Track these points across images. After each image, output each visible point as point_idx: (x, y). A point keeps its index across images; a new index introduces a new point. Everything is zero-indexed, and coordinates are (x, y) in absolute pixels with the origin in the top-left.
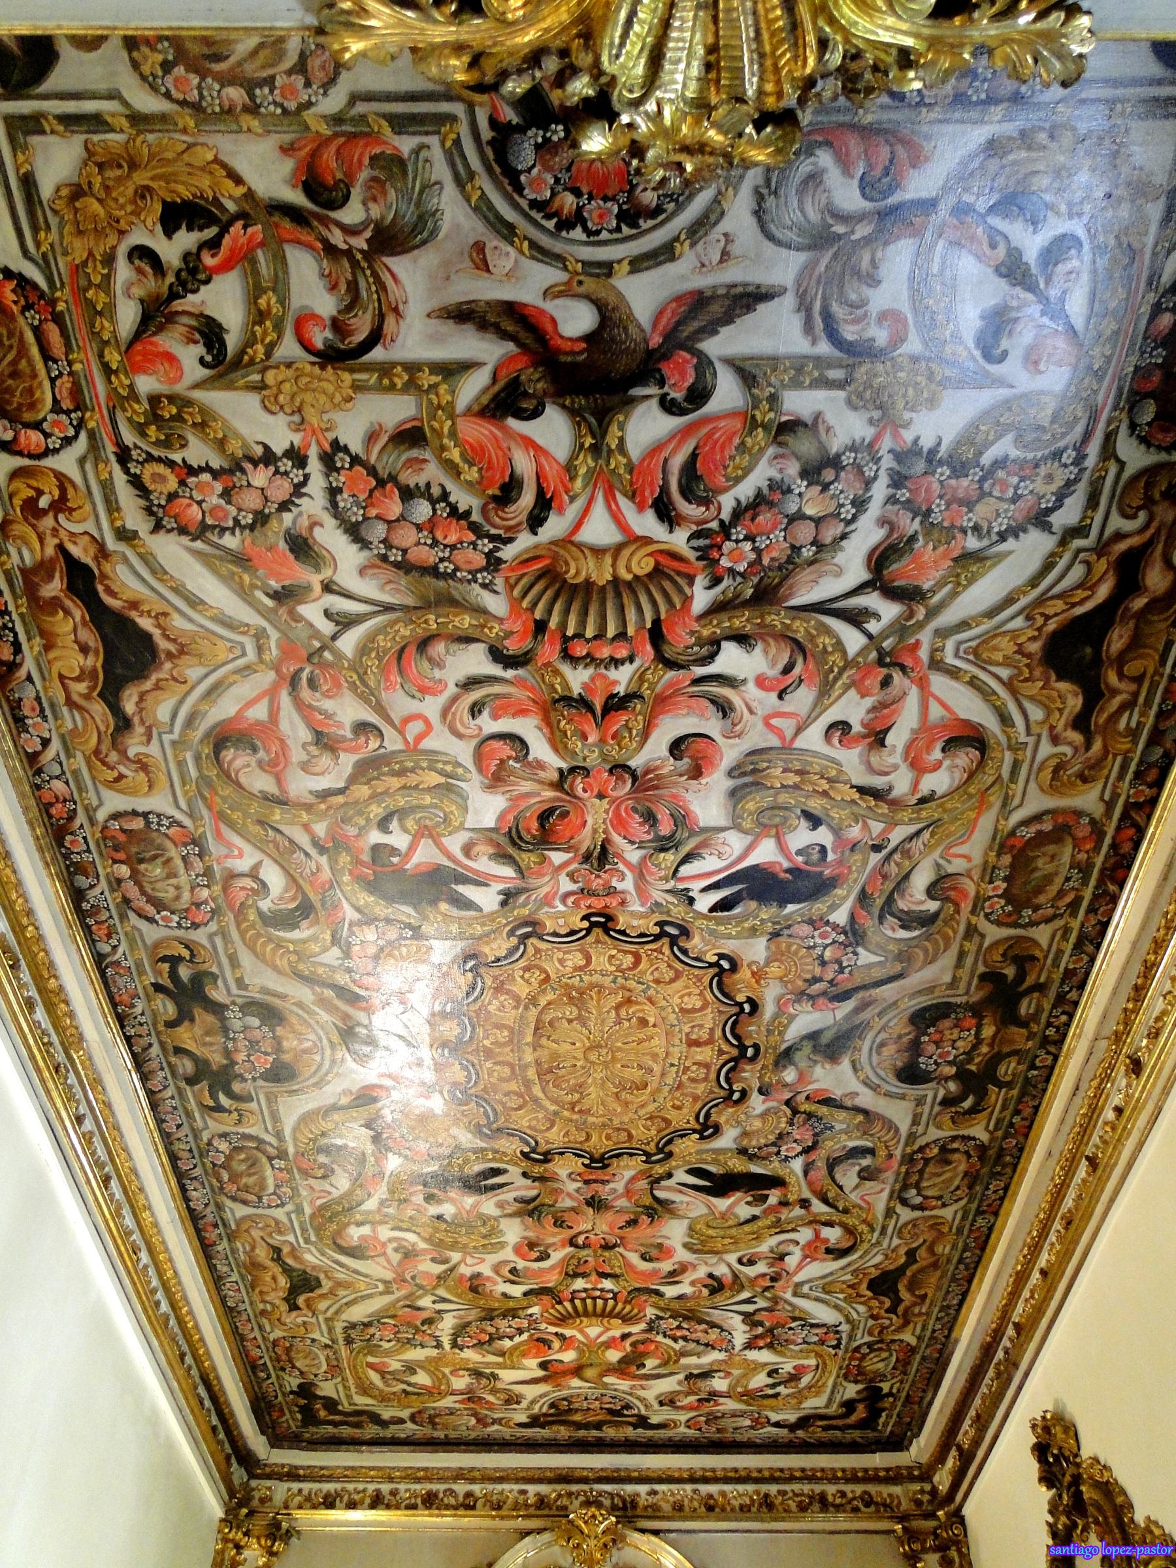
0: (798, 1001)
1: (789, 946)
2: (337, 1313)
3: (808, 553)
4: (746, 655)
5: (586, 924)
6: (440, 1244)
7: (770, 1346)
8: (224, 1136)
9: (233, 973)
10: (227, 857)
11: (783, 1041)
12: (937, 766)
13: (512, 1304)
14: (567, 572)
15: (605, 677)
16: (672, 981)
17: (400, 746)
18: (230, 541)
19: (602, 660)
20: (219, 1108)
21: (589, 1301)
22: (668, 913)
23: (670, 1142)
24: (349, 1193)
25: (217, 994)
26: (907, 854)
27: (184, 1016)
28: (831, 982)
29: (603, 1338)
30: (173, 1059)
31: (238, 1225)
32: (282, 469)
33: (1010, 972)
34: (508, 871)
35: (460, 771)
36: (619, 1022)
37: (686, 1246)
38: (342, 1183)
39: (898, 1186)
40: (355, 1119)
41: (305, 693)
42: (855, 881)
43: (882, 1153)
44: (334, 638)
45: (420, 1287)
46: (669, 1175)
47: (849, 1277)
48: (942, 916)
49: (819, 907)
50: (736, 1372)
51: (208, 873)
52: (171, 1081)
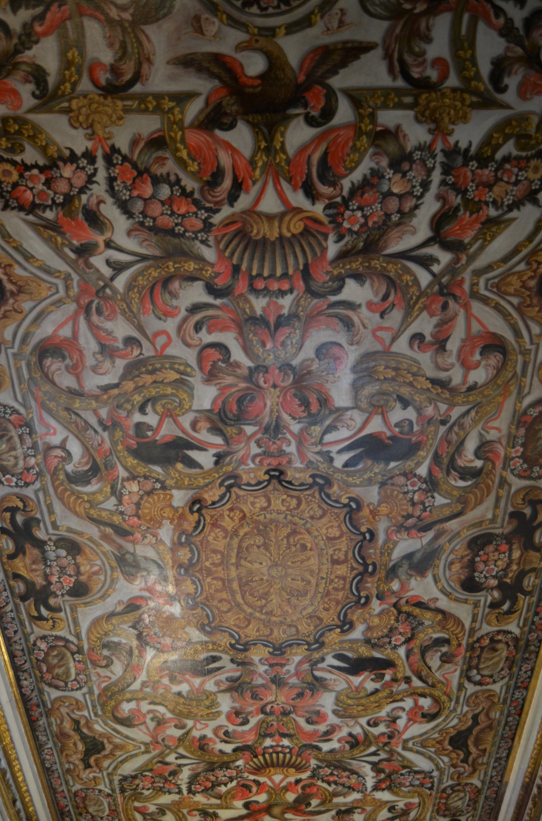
0: (398, 531)
1: (393, 491)
2: (115, 769)
3: (395, 218)
4: (359, 288)
5: (267, 477)
6: (180, 714)
7: (389, 788)
8: (44, 638)
9: (50, 518)
10: (47, 434)
11: (391, 560)
12: (477, 365)
13: (226, 759)
14: (252, 232)
15: (276, 303)
16: (321, 517)
17: (152, 353)
18: (49, 215)
19: (274, 292)
20: (41, 618)
21: (274, 755)
22: (317, 468)
23: (322, 635)
24: (123, 677)
25: (41, 534)
26: (462, 427)
27: (19, 551)
28: (419, 517)
29: (284, 784)
30: (12, 583)
31: (52, 703)
32: (81, 165)
33: (528, 511)
34: (219, 440)
35: (189, 370)
36: (288, 547)
37: (334, 712)
38: (118, 668)
39: (465, 667)
40: (125, 622)
41: (95, 318)
42: (431, 445)
43: (454, 643)
44: (112, 279)
45: (168, 747)
46: (323, 660)
47: (436, 735)
48: (485, 471)
49: (410, 464)
50: (368, 809)
51: (34, 446)
52: (10, 599)
